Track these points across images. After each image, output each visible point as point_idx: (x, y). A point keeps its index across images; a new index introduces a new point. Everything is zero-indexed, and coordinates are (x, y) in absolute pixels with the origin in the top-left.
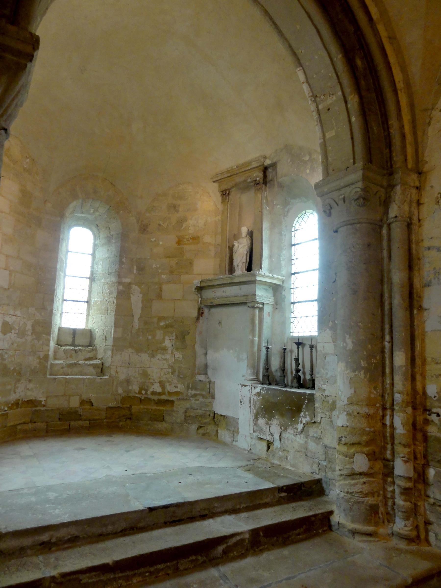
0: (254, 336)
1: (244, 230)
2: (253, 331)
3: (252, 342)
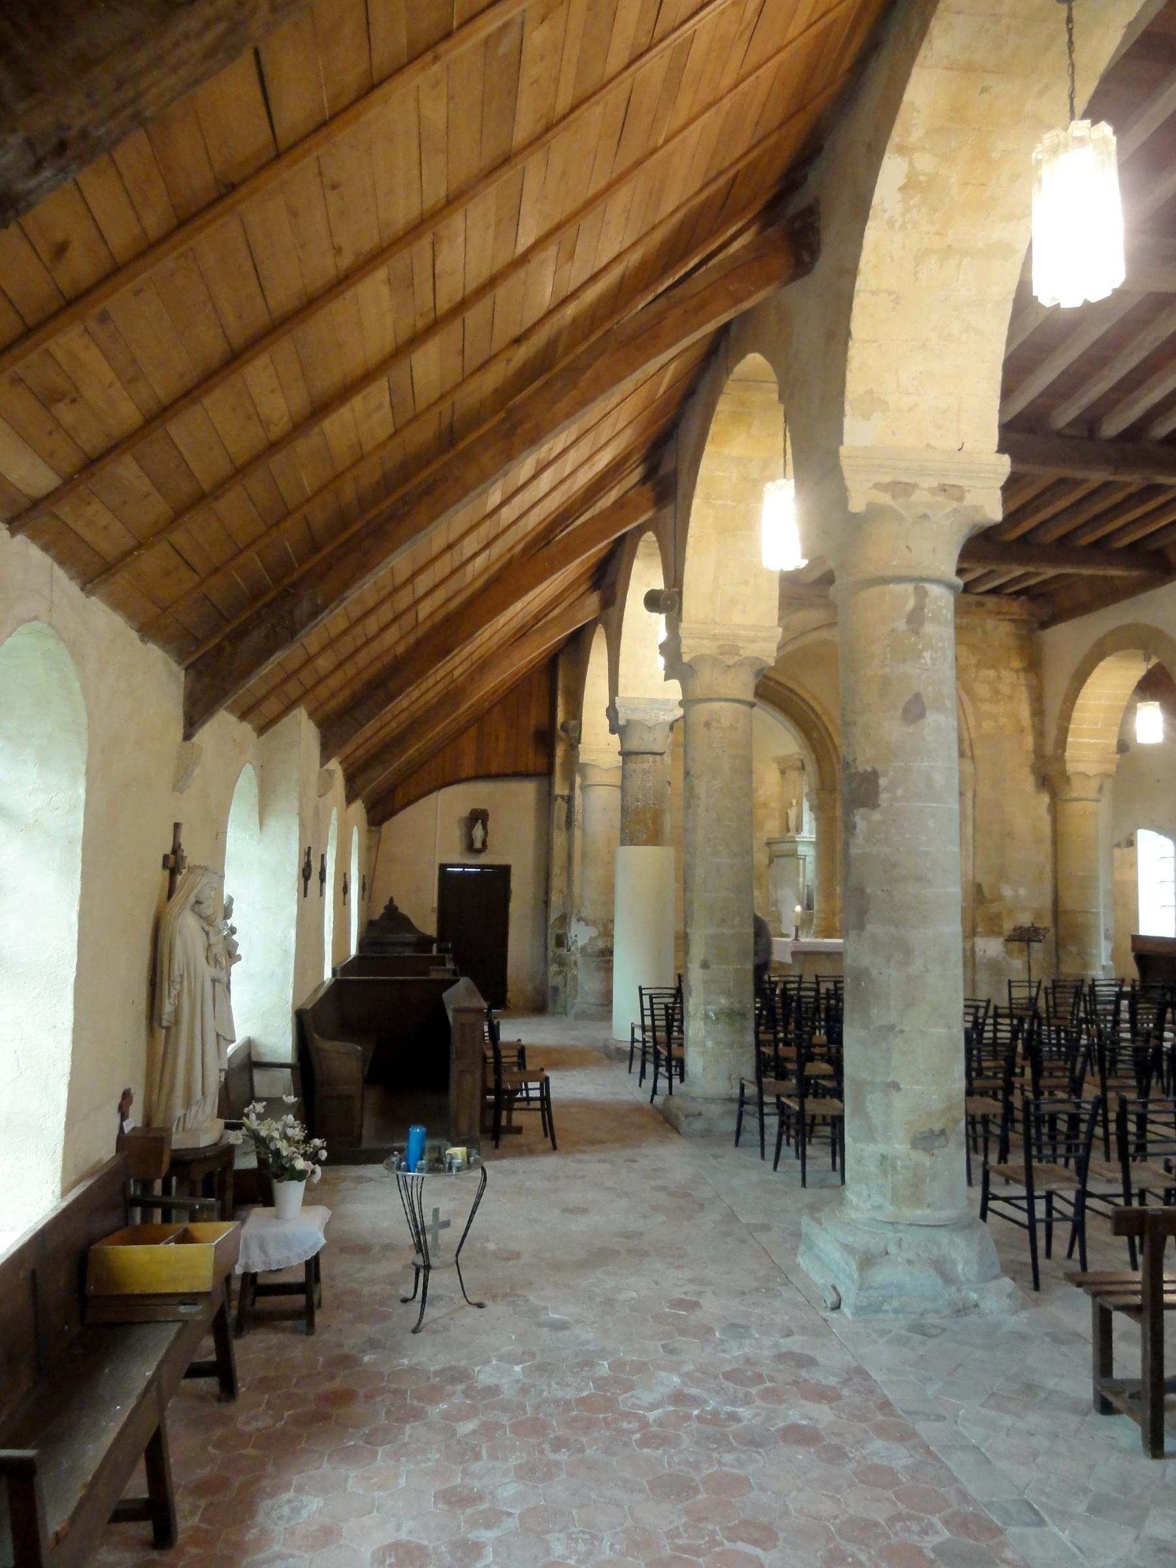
0: (799, 878)
1: (794, 801)
2: (798, 874)
3: (798, 883)
